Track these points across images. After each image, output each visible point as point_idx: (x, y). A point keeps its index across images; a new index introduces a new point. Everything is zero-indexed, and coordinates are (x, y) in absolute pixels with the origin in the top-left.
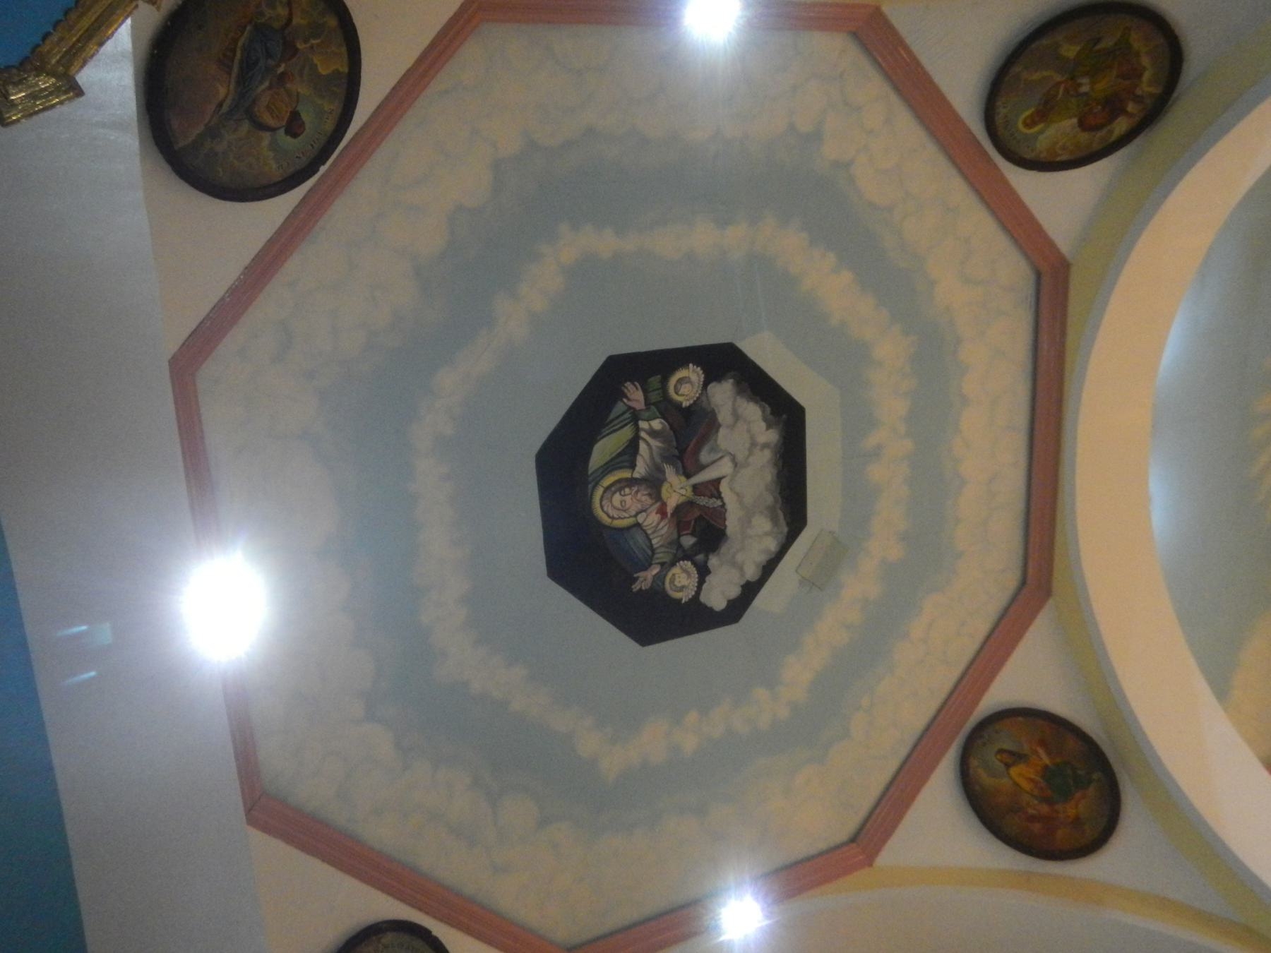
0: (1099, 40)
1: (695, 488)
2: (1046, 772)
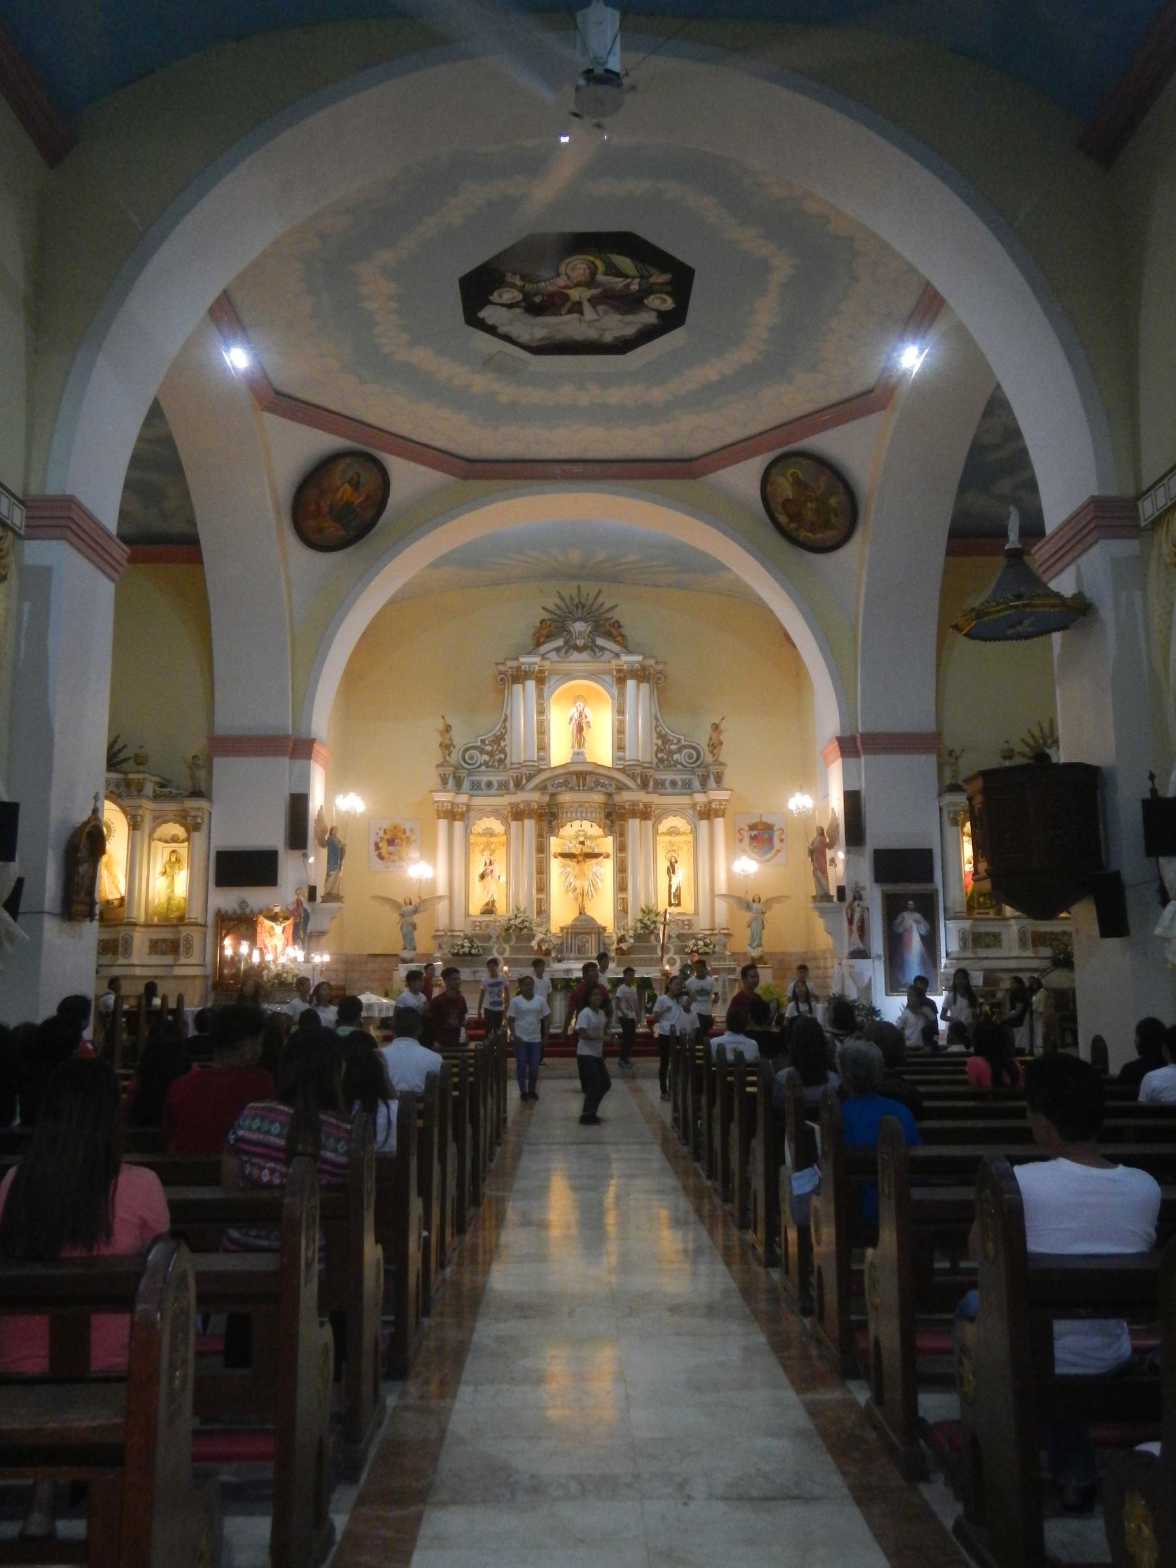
0: (836, 515)
1: (580, 303)
2: (349, 505)
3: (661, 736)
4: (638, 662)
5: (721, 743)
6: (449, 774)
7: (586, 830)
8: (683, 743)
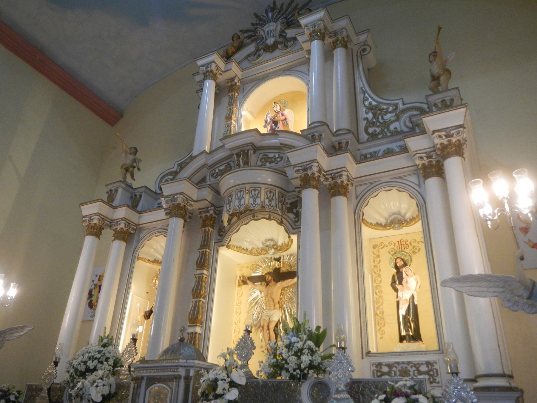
3: (370, 108)
4: (321, 20)
5: (449, 72)
6: (116, 191)
7: (275, 238)
8: (401, 107)
